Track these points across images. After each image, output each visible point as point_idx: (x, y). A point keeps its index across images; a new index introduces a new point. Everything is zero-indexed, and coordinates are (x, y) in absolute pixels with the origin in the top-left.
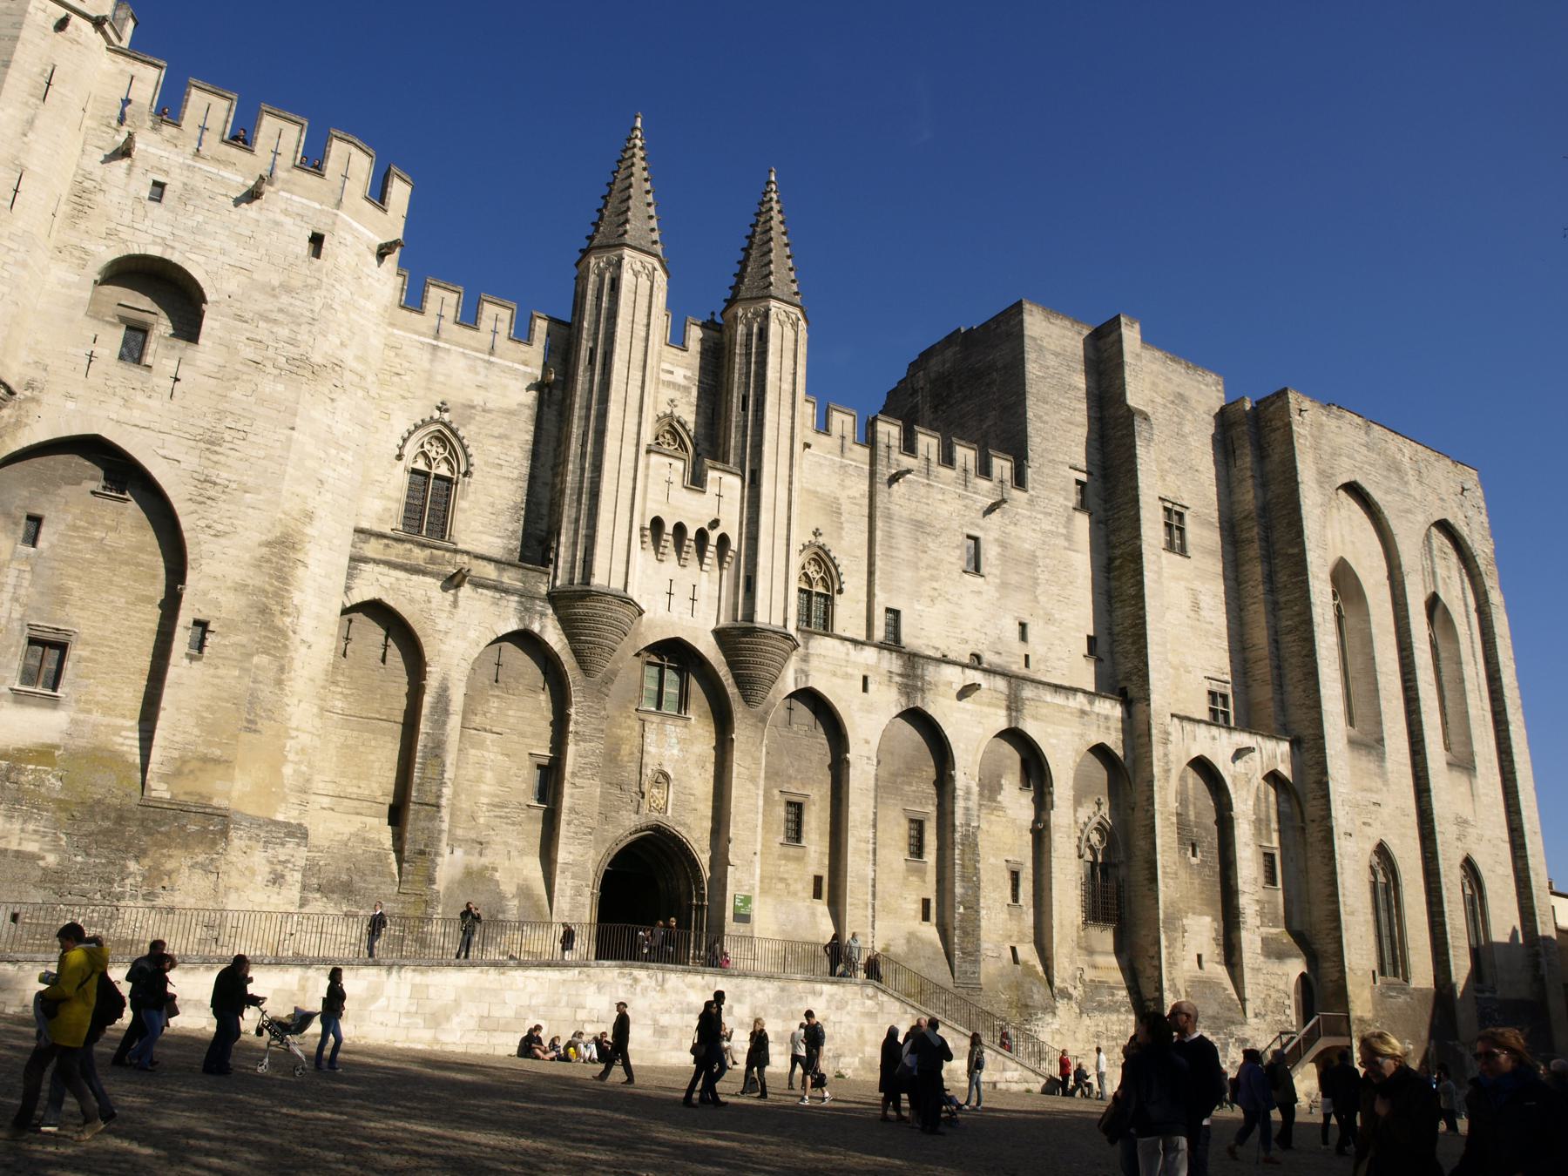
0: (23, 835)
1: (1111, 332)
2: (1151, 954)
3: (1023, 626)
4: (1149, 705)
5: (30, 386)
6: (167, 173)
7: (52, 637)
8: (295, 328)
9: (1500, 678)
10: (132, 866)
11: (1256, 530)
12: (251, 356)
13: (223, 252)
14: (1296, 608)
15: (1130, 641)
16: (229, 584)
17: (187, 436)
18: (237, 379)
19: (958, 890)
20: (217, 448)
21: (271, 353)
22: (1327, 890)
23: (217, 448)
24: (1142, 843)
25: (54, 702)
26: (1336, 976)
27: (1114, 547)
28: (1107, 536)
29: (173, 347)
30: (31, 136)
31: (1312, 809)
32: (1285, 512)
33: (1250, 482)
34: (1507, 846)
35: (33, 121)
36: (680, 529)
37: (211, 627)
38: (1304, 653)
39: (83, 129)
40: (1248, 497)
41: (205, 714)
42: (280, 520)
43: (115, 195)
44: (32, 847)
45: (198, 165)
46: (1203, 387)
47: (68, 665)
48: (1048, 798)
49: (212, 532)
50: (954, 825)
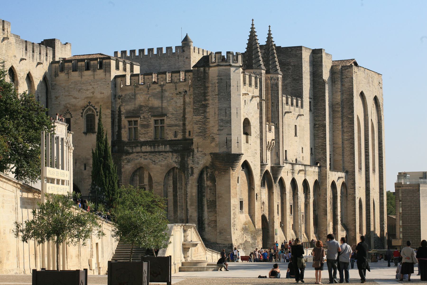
1: (319, 53)
2: (324, 233)
3: (302, 148)
4: (326, 168)
7: (241, 200)
9: (382, 144)
11: (340, 109)
14: (349, 134)
15: (321, 149)
19: (299, 222)
22: (353, 213)
24: (323, 205)
26: (353, 235)
27: (316, 121)
28: (314, 117)
31: (350, 191)
32: (349, 104)
33: (339, 93)
34: (379, 194)
36: (269, 142)
38: (351, 147)
40: (339, 98)
46: (329, 60)
48: (308, 196)
50: (298, 206)
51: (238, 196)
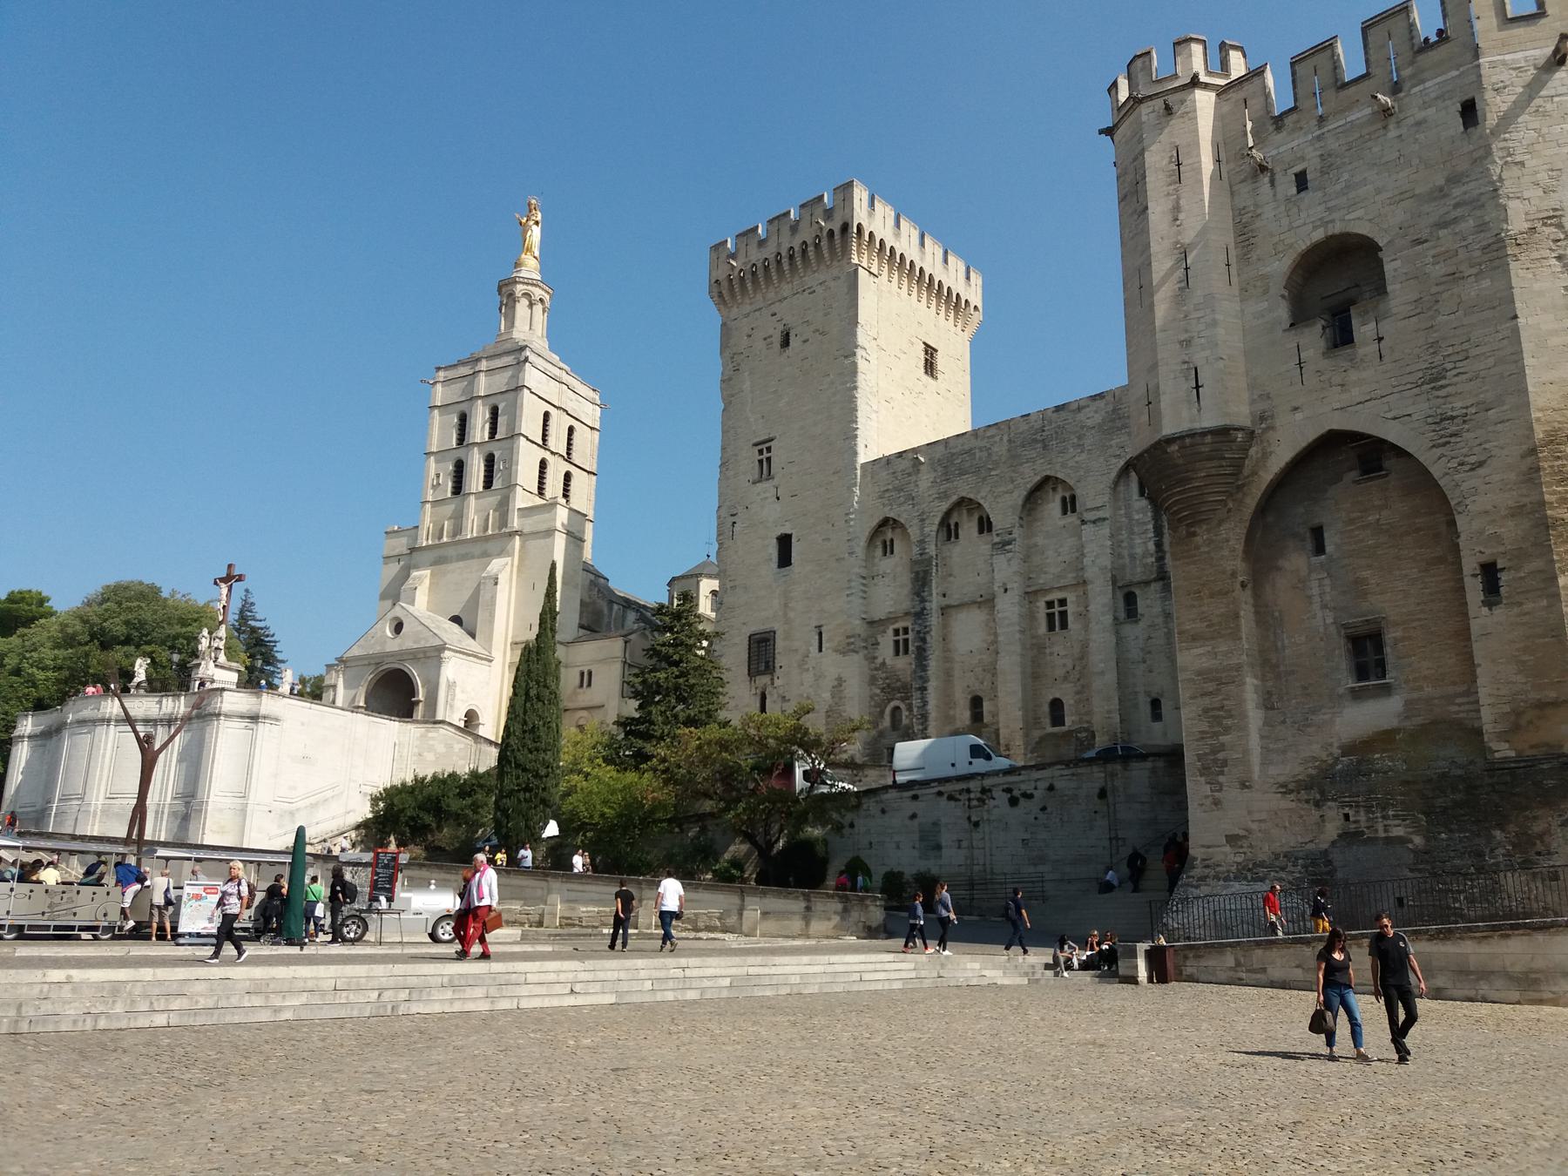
0: (1385, 823)
5: (1262, 419)
6: (1303, 159)
8: (1478, 213)
10: (1498, 834)
12: (1443, 271)
13: (1378, 191)
16: (1503, 512)
17: (1409, 386)
18: (1437, 301)
20: (1443, 382)
21: (1462, 254)
23: (1443, 382)
25: (1386, 690)
29: (1366, 312)
30: (1181, 216)
35: (1178, 203)
37: (1499, 566)
39: (1224, 175)
41: (1525, 658)
42: (1538, 419)
43: (1268, 212)
44: (1398, 831)
45: (1323, 131)
47: (1388, 650)
49: (1467, 468)
51: (1323, 620)
